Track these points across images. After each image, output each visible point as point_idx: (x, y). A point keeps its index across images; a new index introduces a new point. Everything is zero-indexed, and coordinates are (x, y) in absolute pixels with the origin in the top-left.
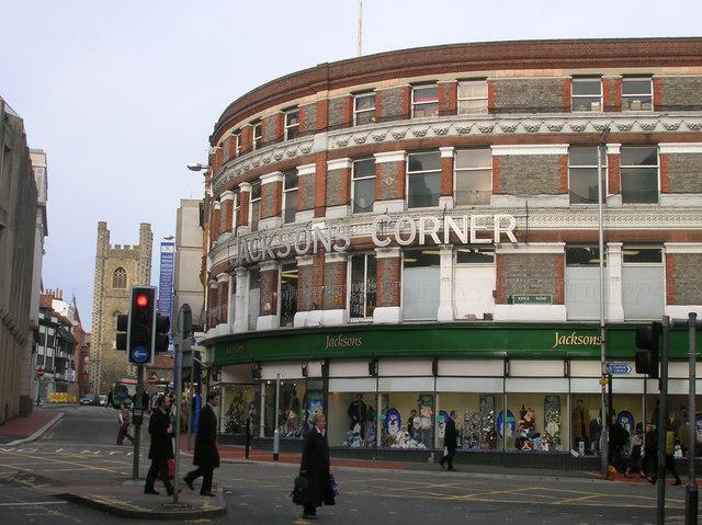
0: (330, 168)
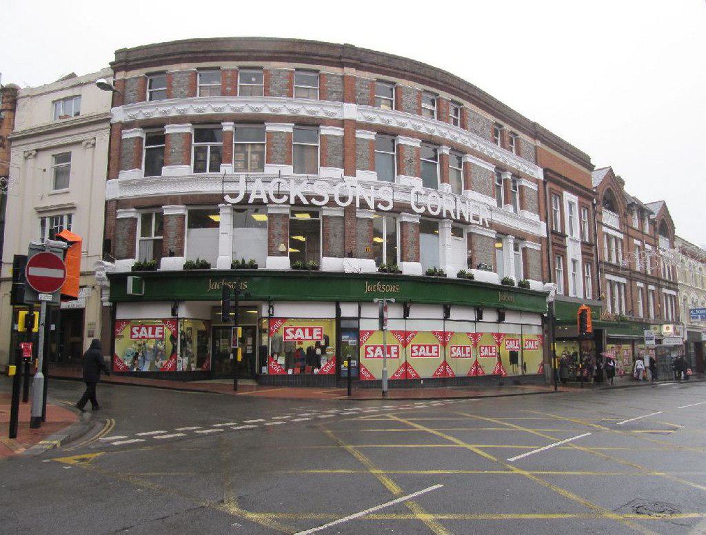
0: (358, 136)
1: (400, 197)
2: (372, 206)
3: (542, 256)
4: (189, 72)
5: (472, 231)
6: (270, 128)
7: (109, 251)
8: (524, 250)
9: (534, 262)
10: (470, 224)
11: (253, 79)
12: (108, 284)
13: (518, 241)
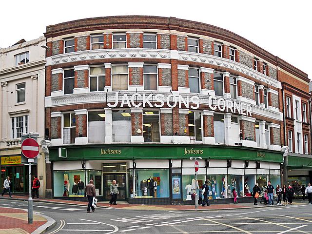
1: (203, 102)
2: (187, 106)
3: (280, 131)
4: (86, 36)
5: (243, 119)
6: (131, 65)
7: (48, 135)
8: (271, 128)
9: (276, 135)
10: (242, 115)
11: (121, 39)
12: (48, 152)
13: (267, 123)
